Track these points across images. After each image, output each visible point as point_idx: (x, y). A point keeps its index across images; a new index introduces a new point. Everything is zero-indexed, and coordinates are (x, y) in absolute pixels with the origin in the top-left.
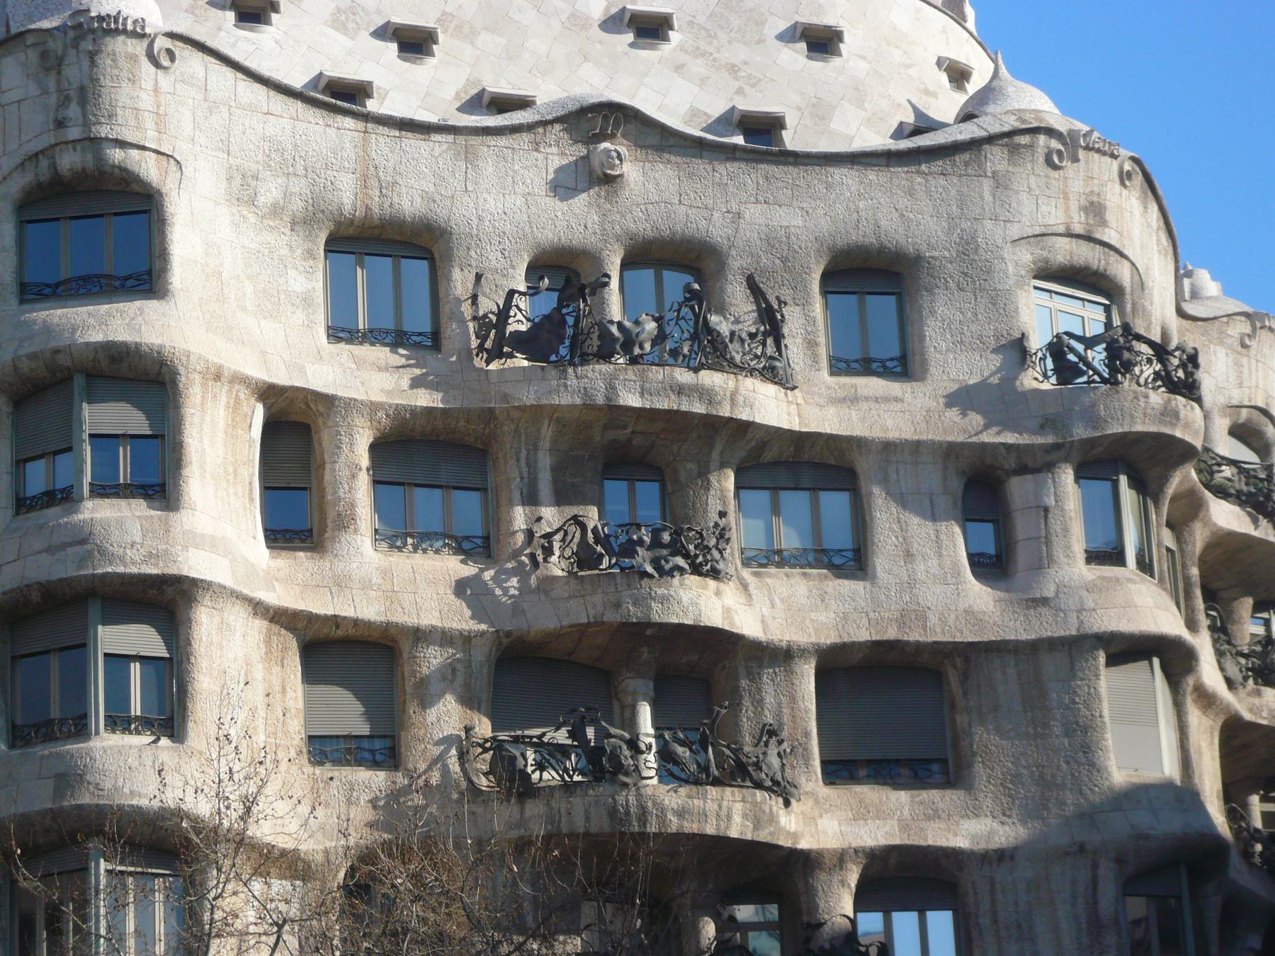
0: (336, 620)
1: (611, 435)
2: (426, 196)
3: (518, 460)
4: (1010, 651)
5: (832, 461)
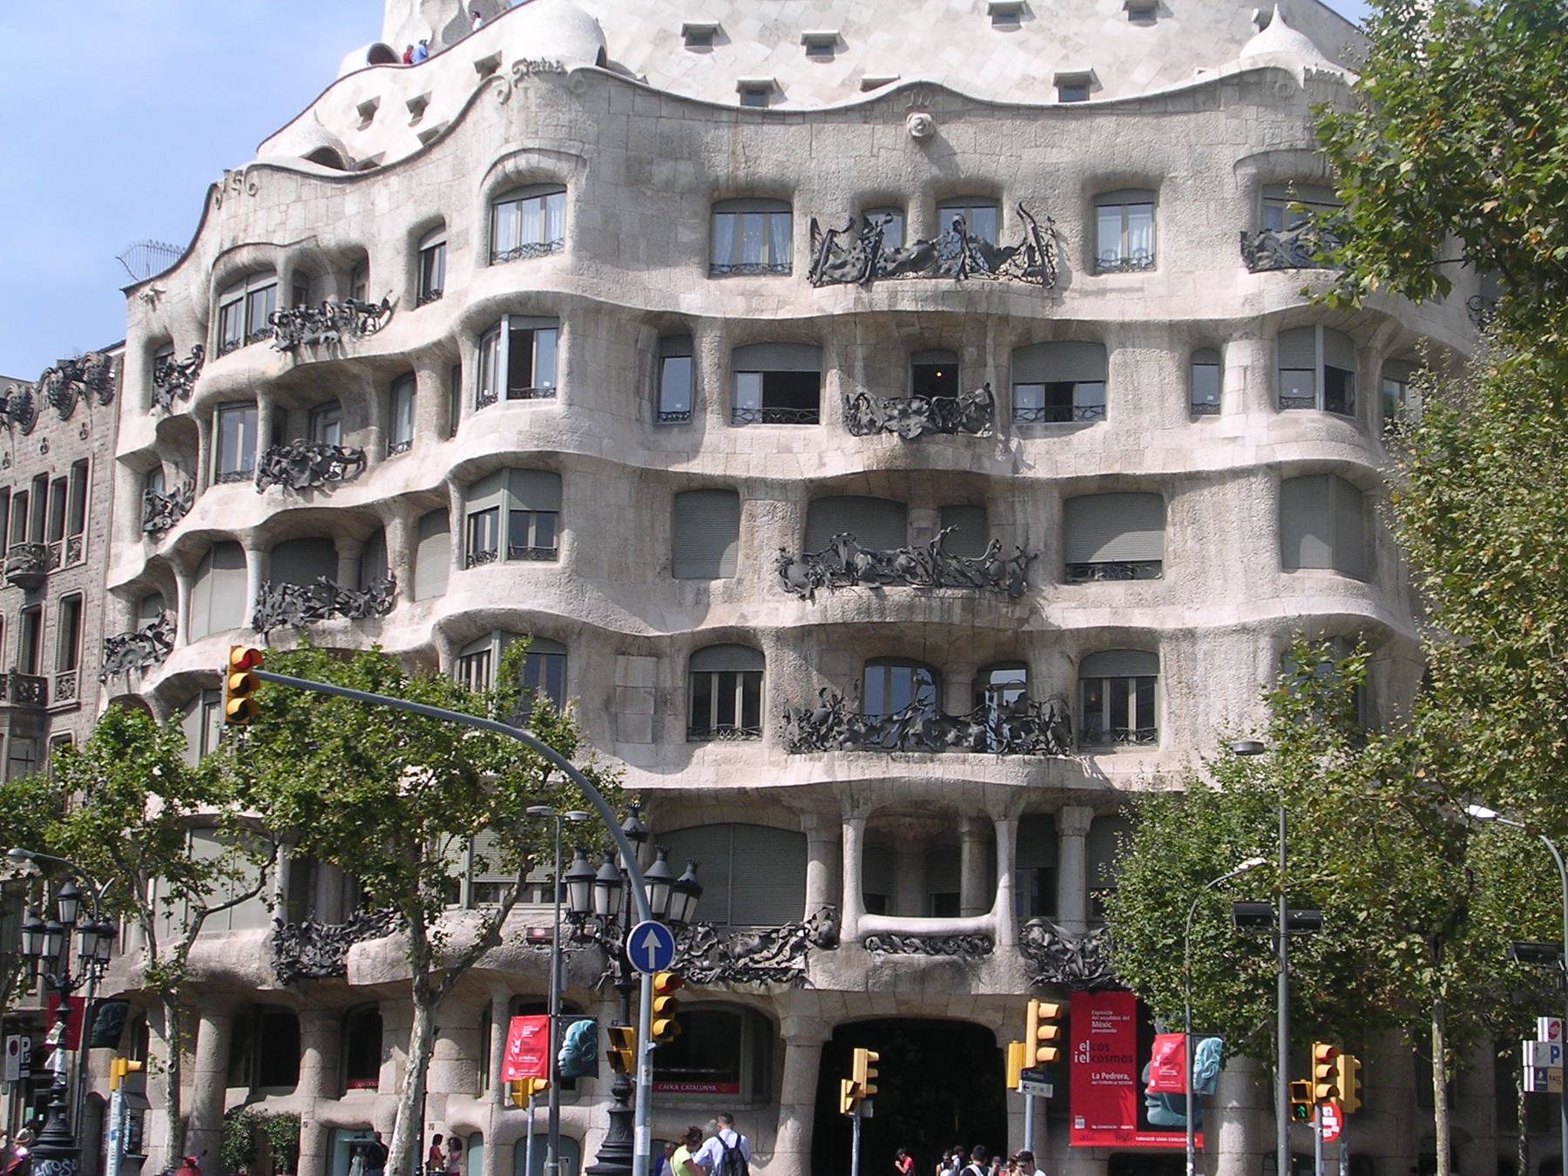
1: (905, 331)
2: (780, 164)
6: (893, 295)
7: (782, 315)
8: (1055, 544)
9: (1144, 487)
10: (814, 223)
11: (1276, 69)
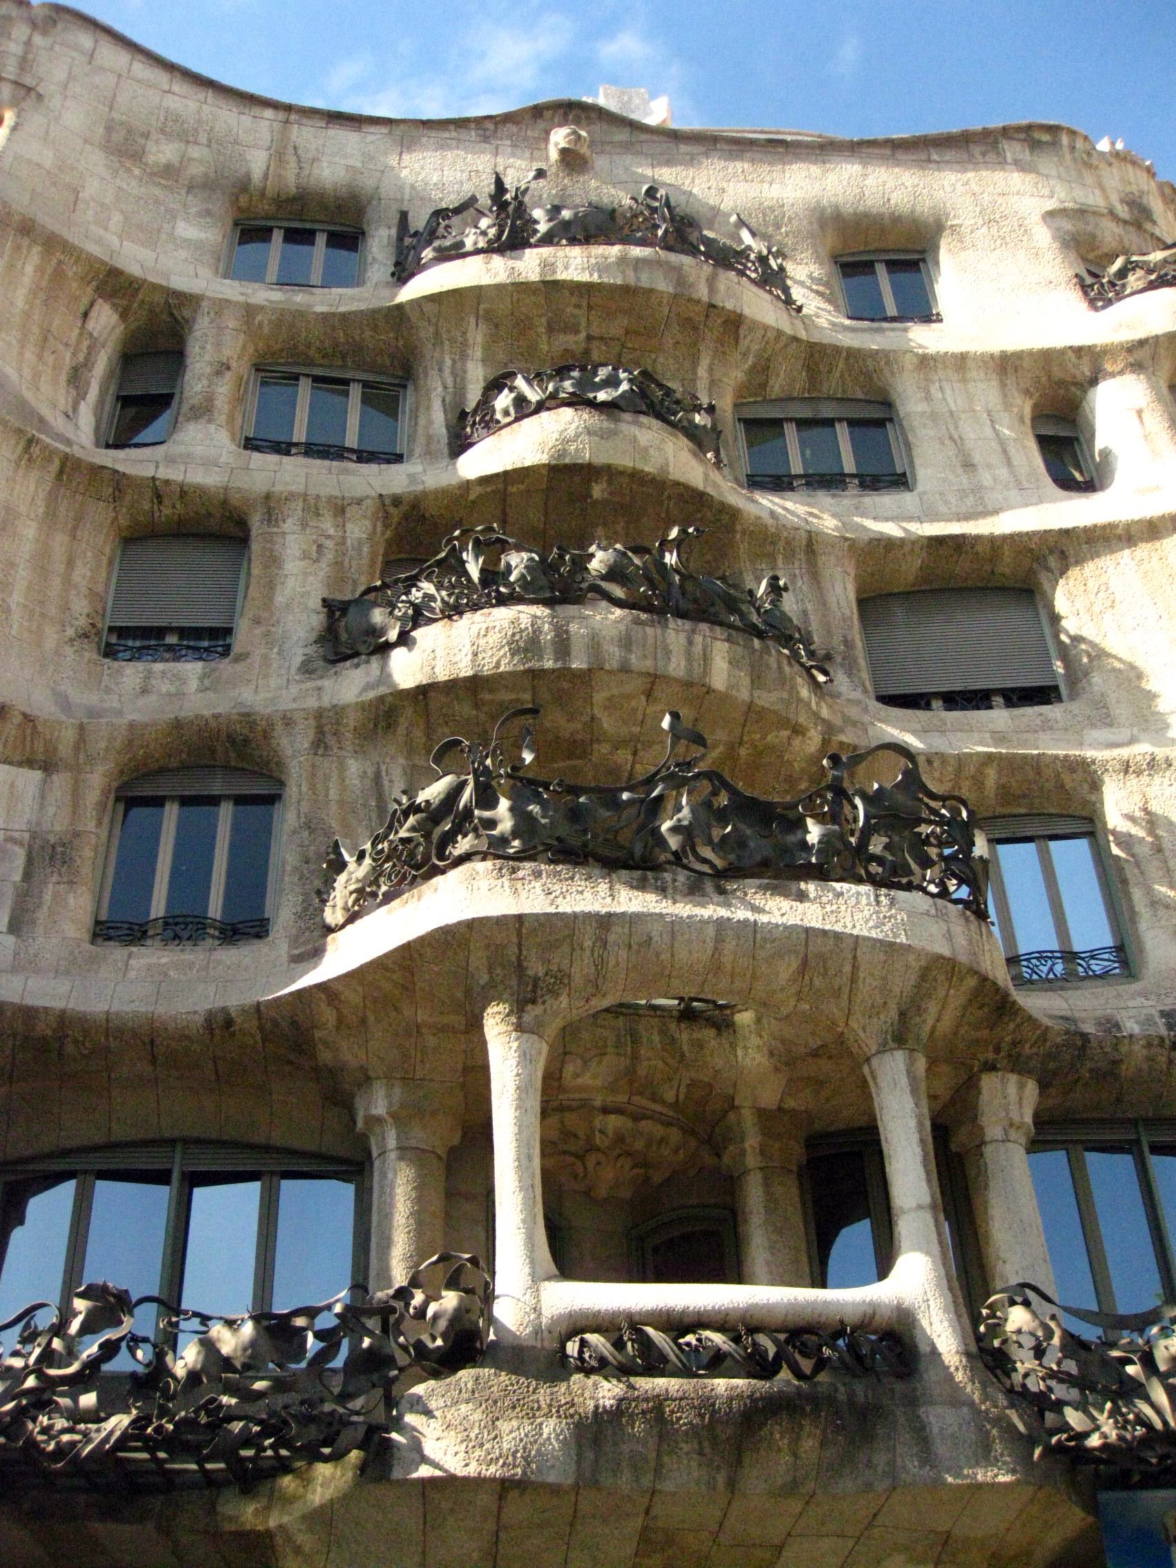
0: (157, 490)
3: (440, 370)
4: (1120, 538)
5: (861, 396)
6: (546, 265)
7: (342, 309)
8: (859, 645)
9: (1006, 565)
10: (404, 216)
11: (1072, 133)
